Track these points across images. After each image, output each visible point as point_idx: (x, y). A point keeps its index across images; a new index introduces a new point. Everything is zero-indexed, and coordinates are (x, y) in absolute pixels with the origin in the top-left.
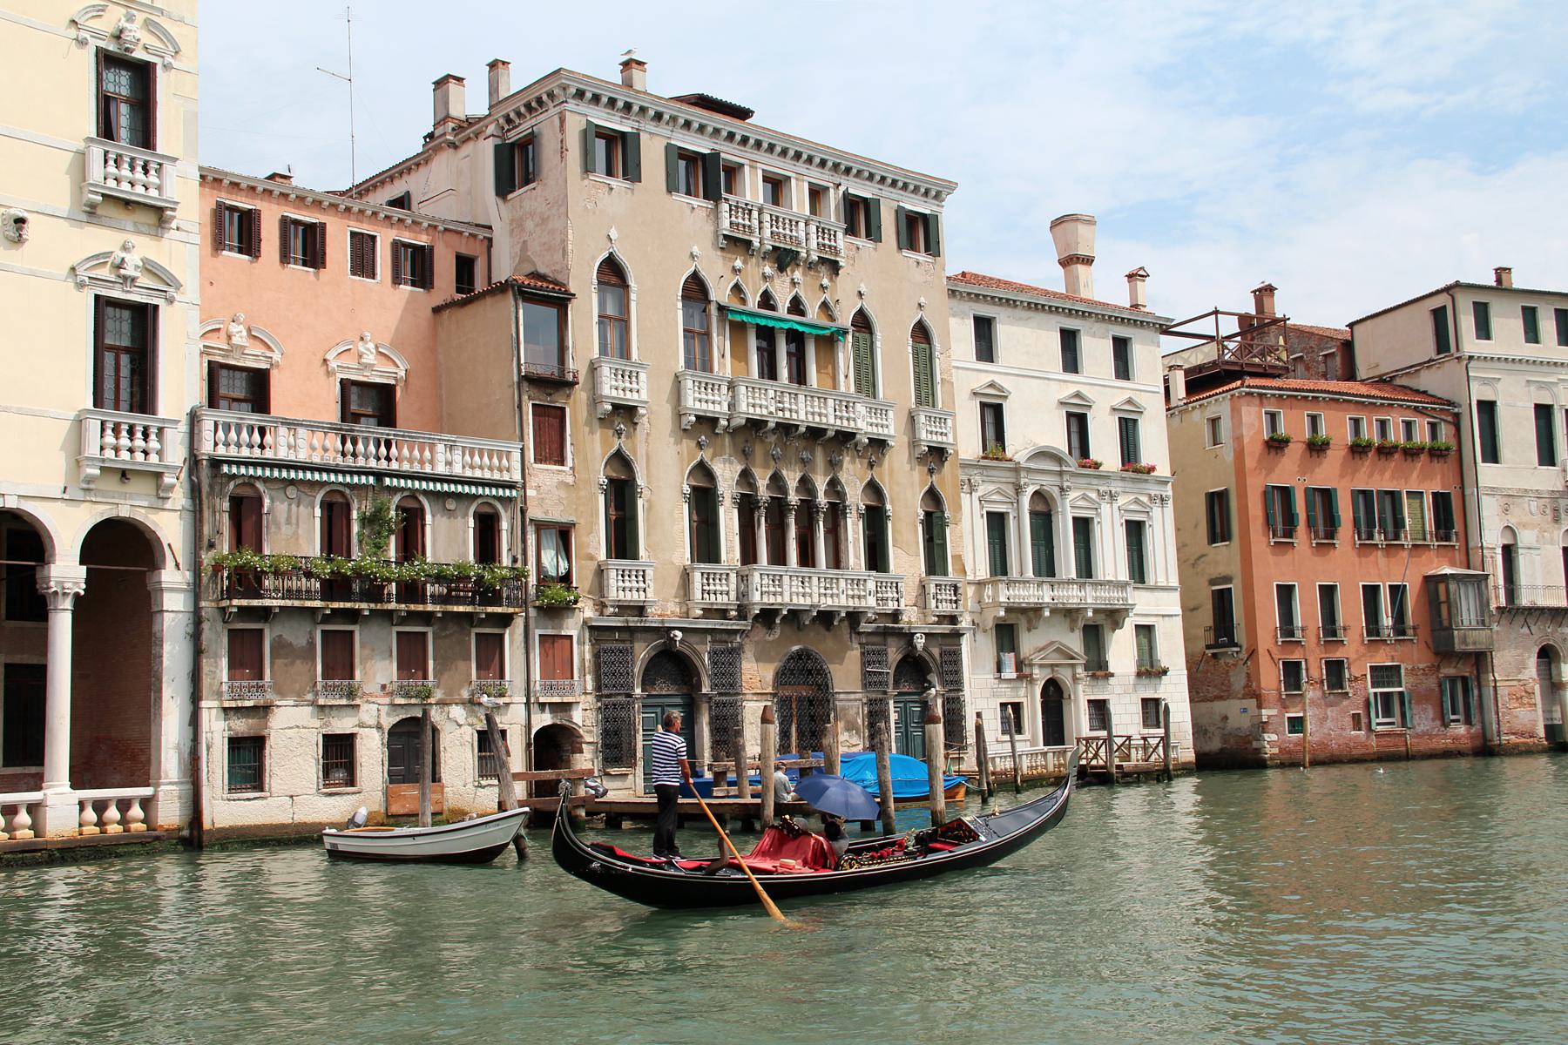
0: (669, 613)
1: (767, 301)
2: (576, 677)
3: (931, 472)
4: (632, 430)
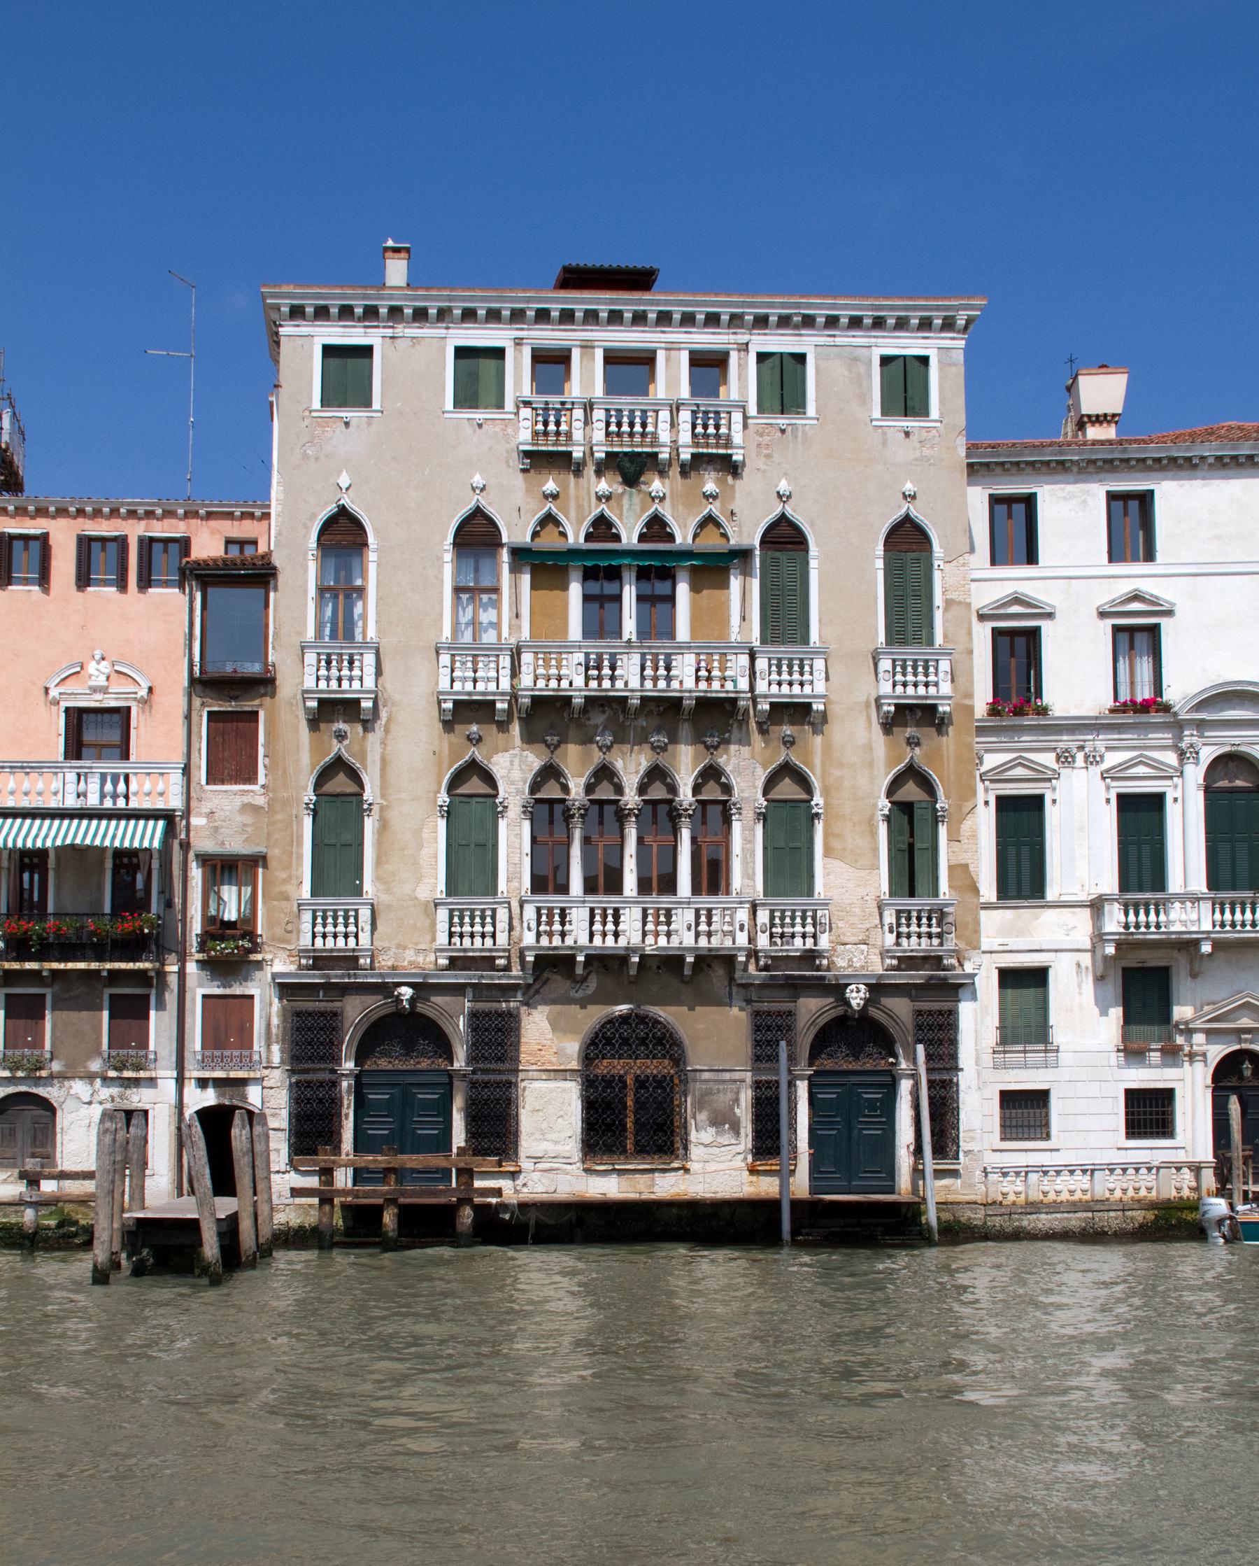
0: (406, 963)
1: (602, 528)
2: (256, 1047)
3: (913, 742)
4: (360, 729)
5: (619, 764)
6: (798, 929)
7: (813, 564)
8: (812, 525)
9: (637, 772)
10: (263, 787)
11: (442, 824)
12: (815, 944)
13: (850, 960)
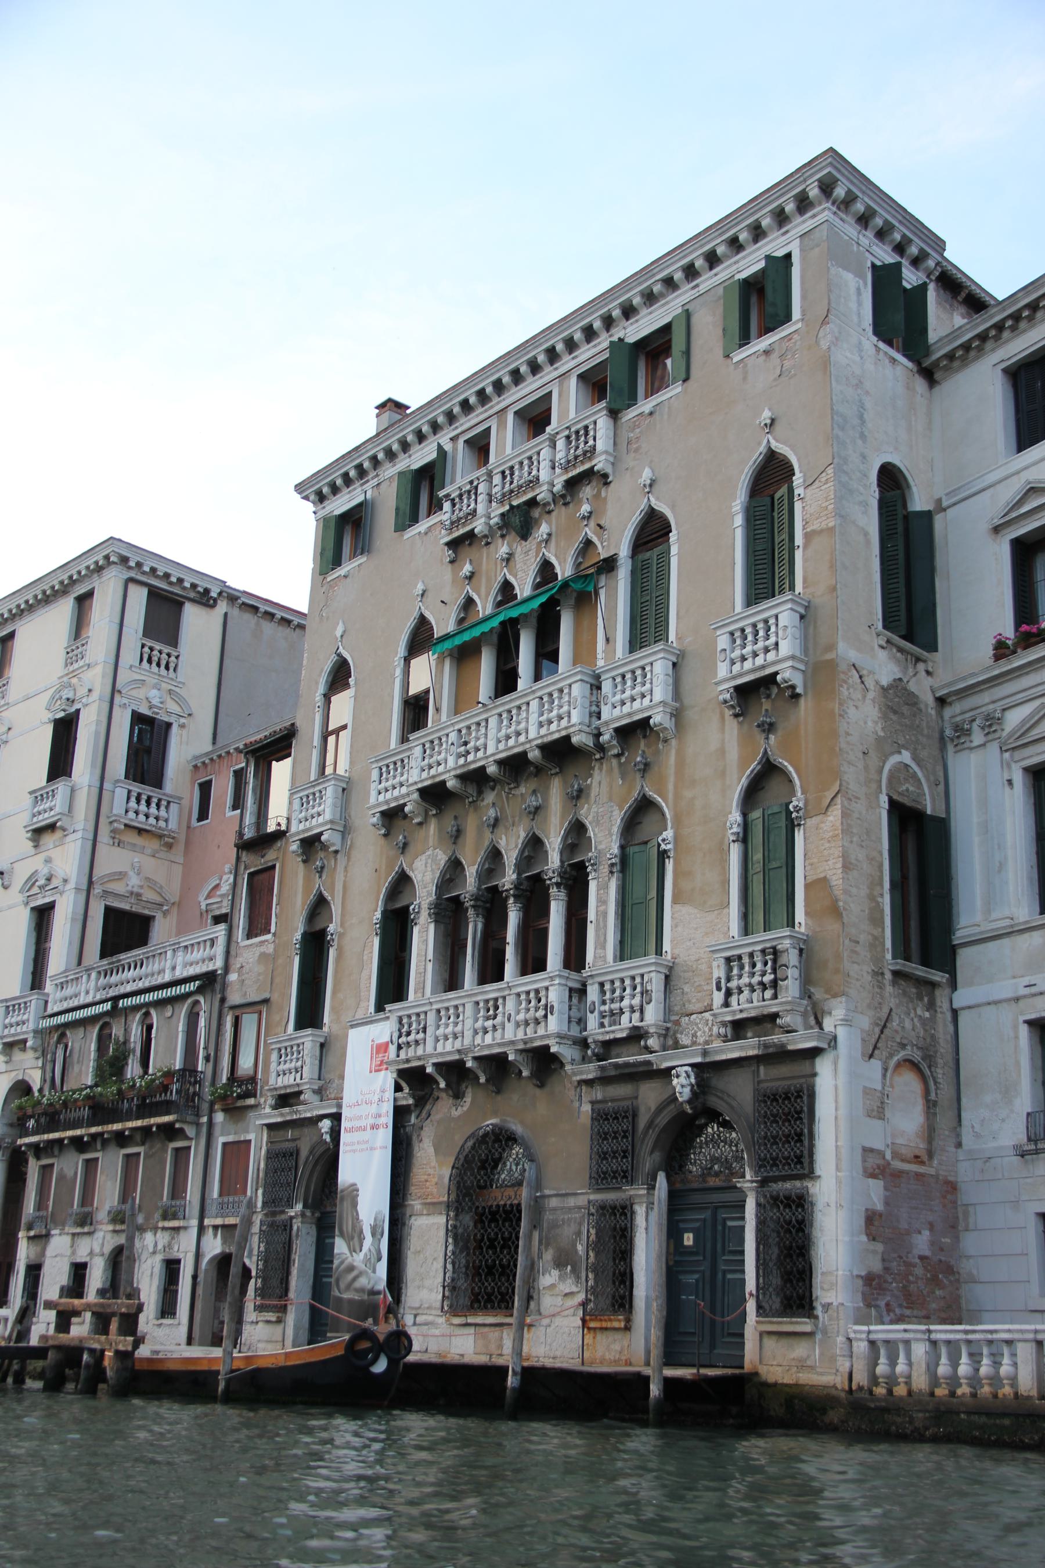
5: (502, 844)
6: (626, 1002)
7: (674, 550)
8: (673, 508)
9: (516, 846)
10: (274, 935)
11: (376, 941)
12: (642, 1020)
13: (694, 1035)
